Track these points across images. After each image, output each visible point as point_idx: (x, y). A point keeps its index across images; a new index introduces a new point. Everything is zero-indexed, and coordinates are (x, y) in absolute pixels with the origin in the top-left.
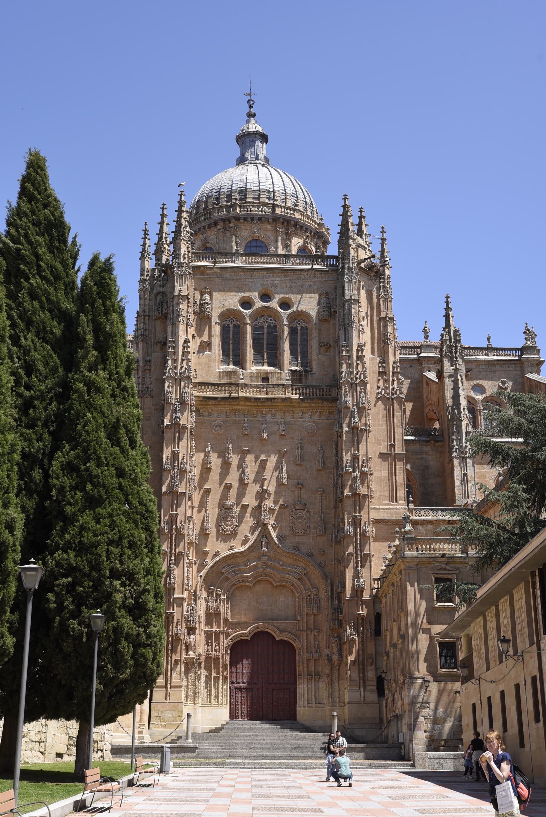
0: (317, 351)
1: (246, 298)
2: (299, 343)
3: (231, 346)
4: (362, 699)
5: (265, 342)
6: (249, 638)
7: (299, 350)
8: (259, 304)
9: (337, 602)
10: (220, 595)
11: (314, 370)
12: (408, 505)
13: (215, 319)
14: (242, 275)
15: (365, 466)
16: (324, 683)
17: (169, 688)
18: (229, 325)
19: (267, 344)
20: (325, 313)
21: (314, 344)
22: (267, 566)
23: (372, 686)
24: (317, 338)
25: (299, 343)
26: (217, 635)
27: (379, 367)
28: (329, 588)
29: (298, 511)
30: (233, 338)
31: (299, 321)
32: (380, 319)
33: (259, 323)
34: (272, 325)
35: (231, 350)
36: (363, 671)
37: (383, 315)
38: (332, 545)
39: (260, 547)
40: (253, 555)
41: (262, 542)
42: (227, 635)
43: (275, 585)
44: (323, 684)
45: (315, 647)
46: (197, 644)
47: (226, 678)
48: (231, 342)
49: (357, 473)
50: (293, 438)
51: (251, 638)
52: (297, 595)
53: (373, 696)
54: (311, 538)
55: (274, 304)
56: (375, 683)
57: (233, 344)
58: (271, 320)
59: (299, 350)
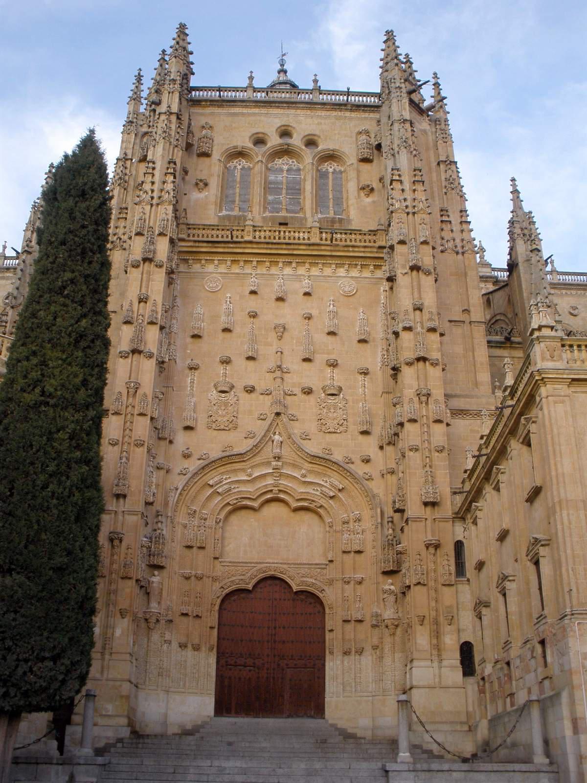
0: (356, 194)
1: (260, 135)
2: (331, 189)
3: (238, 190)
4: (437, 680)
5: (285, 187)
6: (250, 587)
7: (331, 196)
8: (274, 141)
9: (391, 531)
10: (205, 519)
11: (351, 217)
12: (493, 393)
13: (216, 155)
14: (256, 110)
15: (430, 319)
16: (370, 658)
17: (107, 657)
18: (235, 167)
19: (287, 189)
20: (365, 150)
21: (352, 187)
22: (281, 475)
23: (454, 658)
24: (356, 180)
25: (331, 189)
26: (199, 578)
27: (442, 216)
28: (379, 510)
29: (329, 397)
30: (240, 182)
31: (331, 164)
32: (438, 164)
33: (276, 164)
34: (294, 168)
35: (238, 194)
36: (437, 634)
37: (443, 158)
38: (381, 448)
39: (270, 449)
40: (257, 460)
41: (273, 441)
42: (215, 579)
43: (295, 505)
44: (367, 660)
45: (355, 601)
46: (164, 593)
47: (211, 649)
48: (238, 186)
49: (419, 329)
50: (322, 299)
51: (255, 586)
52: (328, 520)
53: (456, 675)
54: (349, 436)
55: (297, 141)
56: (457, 655)
57: (241, 188)
58: (293, 162)
59: (331, 196)
